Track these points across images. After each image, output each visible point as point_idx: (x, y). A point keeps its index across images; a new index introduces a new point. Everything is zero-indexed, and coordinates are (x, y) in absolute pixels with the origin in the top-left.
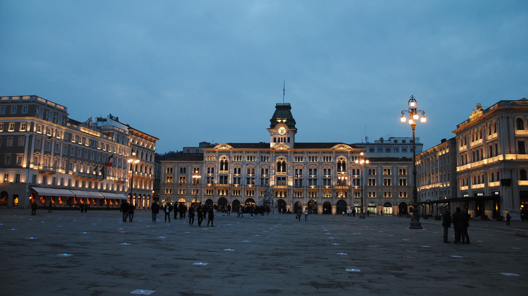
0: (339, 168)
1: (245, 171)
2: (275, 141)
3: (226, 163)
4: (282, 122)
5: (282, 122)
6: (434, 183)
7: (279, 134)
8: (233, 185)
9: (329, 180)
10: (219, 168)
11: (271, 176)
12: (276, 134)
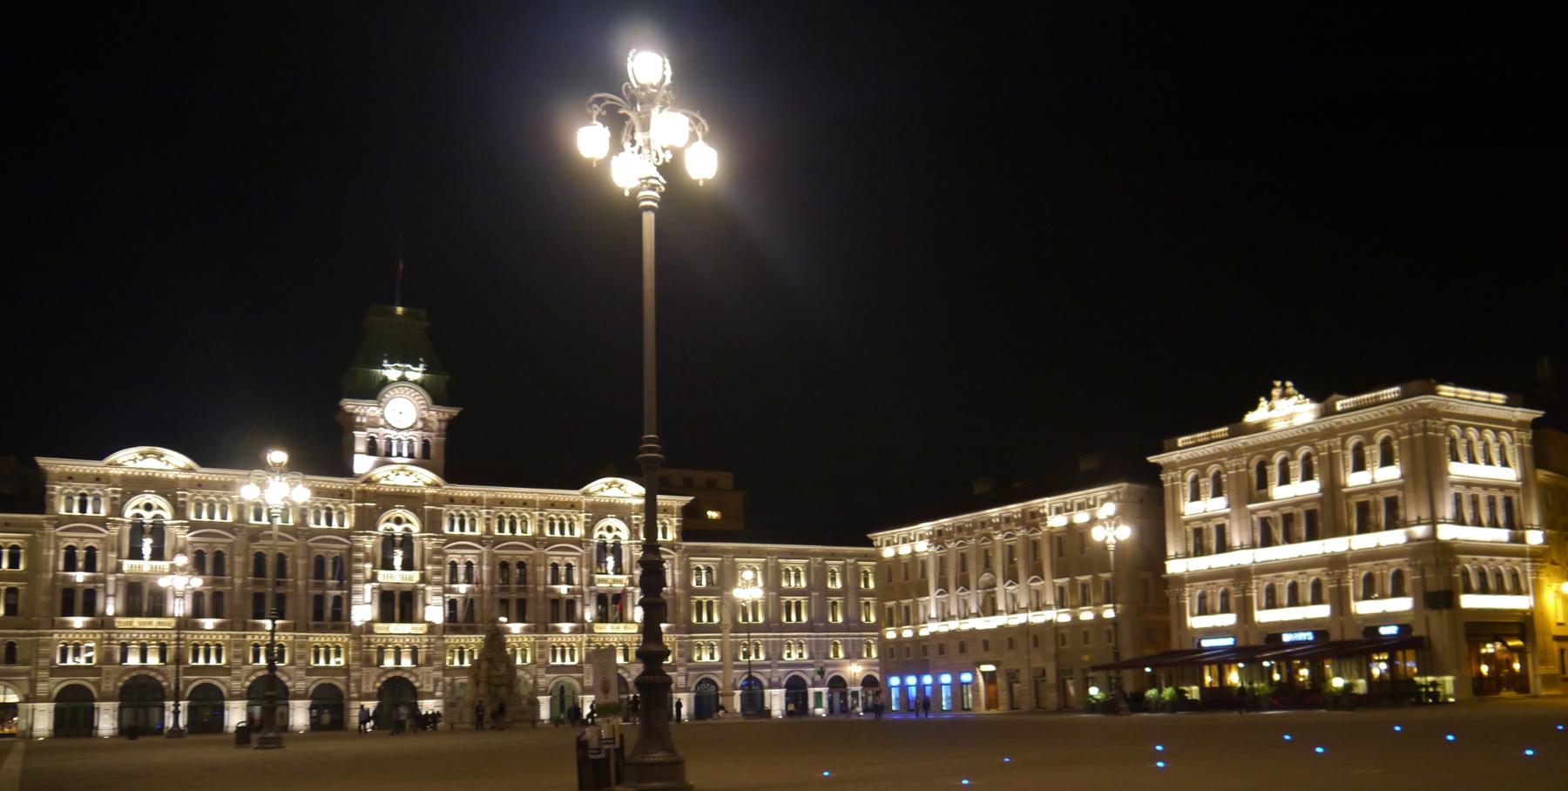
0: (601, 561)
1: (246, 566)
2: (372, 449)
3: (158, 530)
4: (403, 379)
5: (403, 379)
6: (1026, 610)
7: (388, 425)
8: (184, 624)
9: (571, 604)
10: (126, 551)
11: (356, 587)
12: (377, 426)
